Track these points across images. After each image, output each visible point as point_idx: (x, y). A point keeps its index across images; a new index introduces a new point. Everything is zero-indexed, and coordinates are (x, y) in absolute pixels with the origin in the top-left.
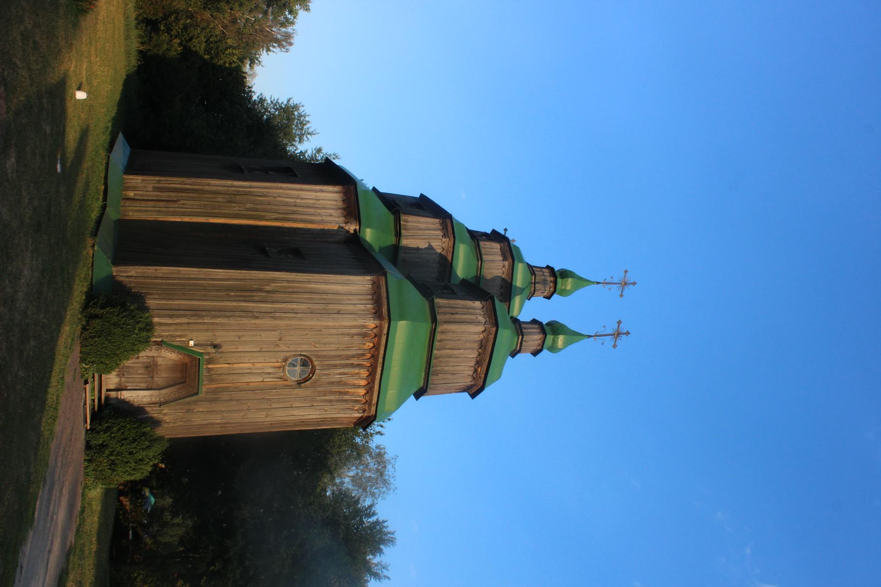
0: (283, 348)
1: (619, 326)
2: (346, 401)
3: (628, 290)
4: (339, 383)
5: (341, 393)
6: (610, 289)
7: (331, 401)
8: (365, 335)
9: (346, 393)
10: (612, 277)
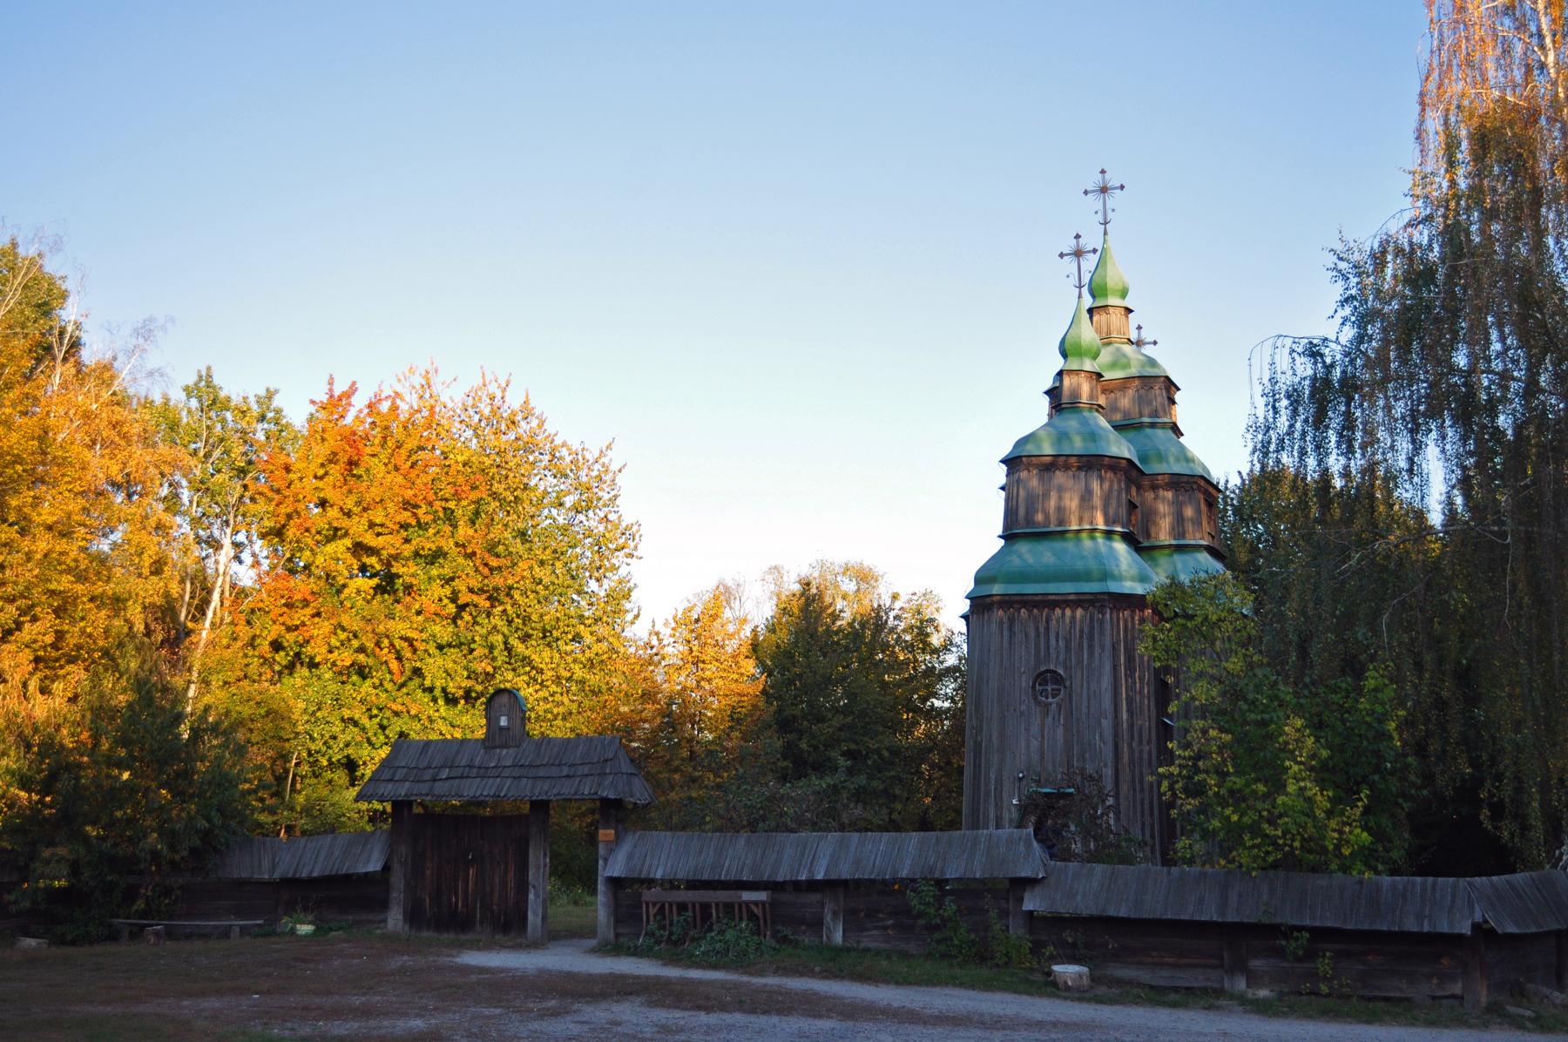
0: (1023, 707)
1: (1067, 255)
2: (1092, 628)
3: (1114, 181)
4: (1068, 641)
5: (1081, 637)
6: (1113, 210)
7: (1091, 647)
8: (1011, 621)
9: (1082, 631)
10: (1096, 212)
